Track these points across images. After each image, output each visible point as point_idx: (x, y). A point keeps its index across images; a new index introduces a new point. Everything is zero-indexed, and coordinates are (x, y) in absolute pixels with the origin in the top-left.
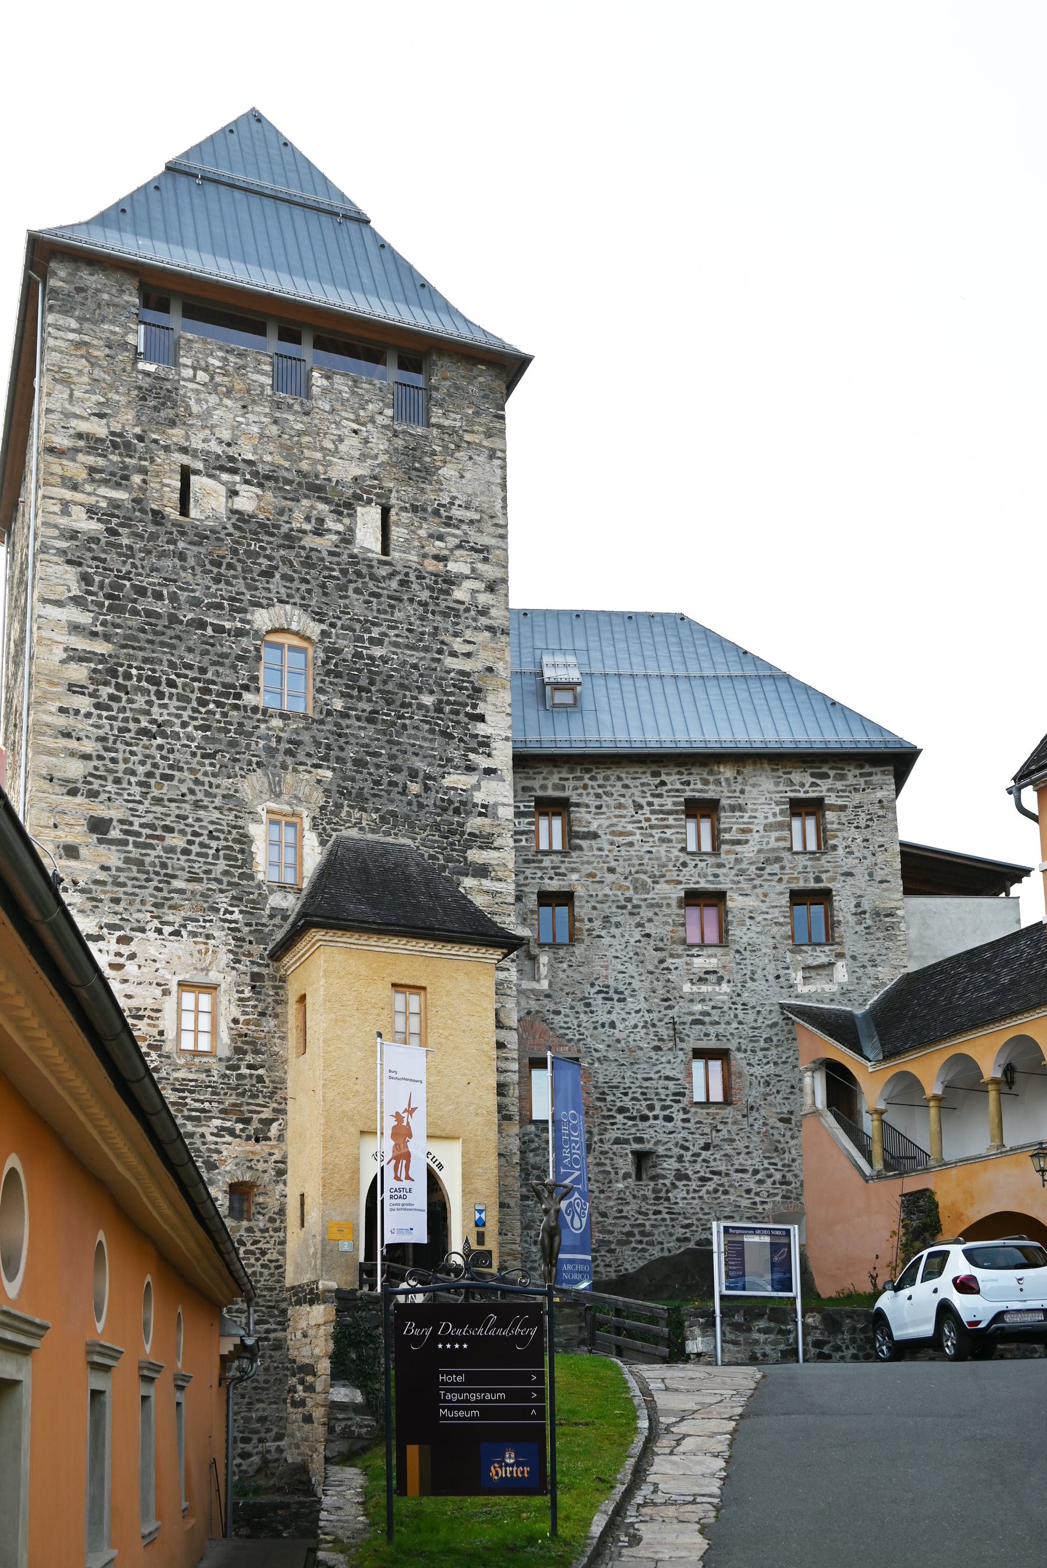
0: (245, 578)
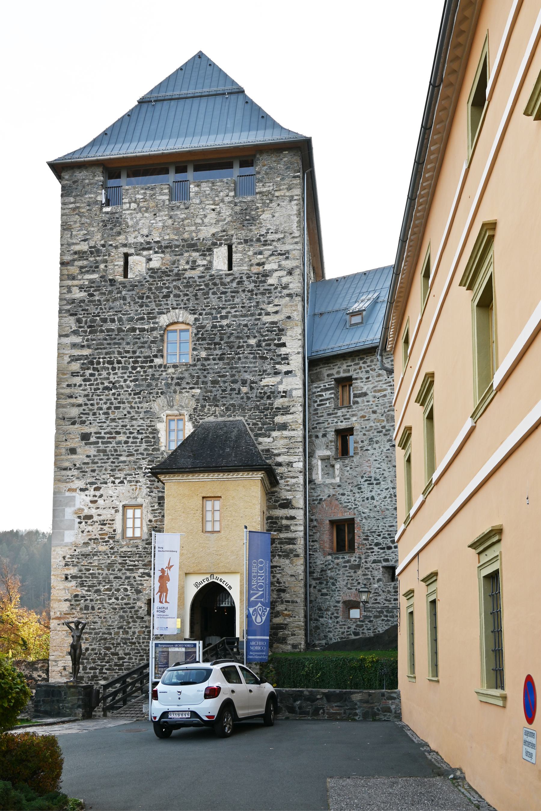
0: (155, 301)
